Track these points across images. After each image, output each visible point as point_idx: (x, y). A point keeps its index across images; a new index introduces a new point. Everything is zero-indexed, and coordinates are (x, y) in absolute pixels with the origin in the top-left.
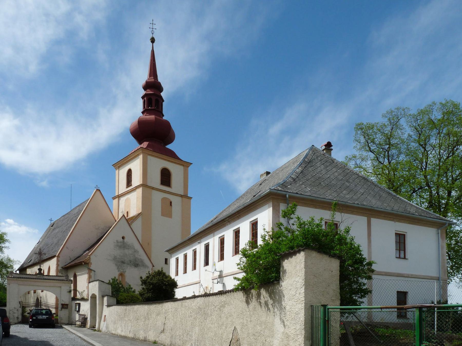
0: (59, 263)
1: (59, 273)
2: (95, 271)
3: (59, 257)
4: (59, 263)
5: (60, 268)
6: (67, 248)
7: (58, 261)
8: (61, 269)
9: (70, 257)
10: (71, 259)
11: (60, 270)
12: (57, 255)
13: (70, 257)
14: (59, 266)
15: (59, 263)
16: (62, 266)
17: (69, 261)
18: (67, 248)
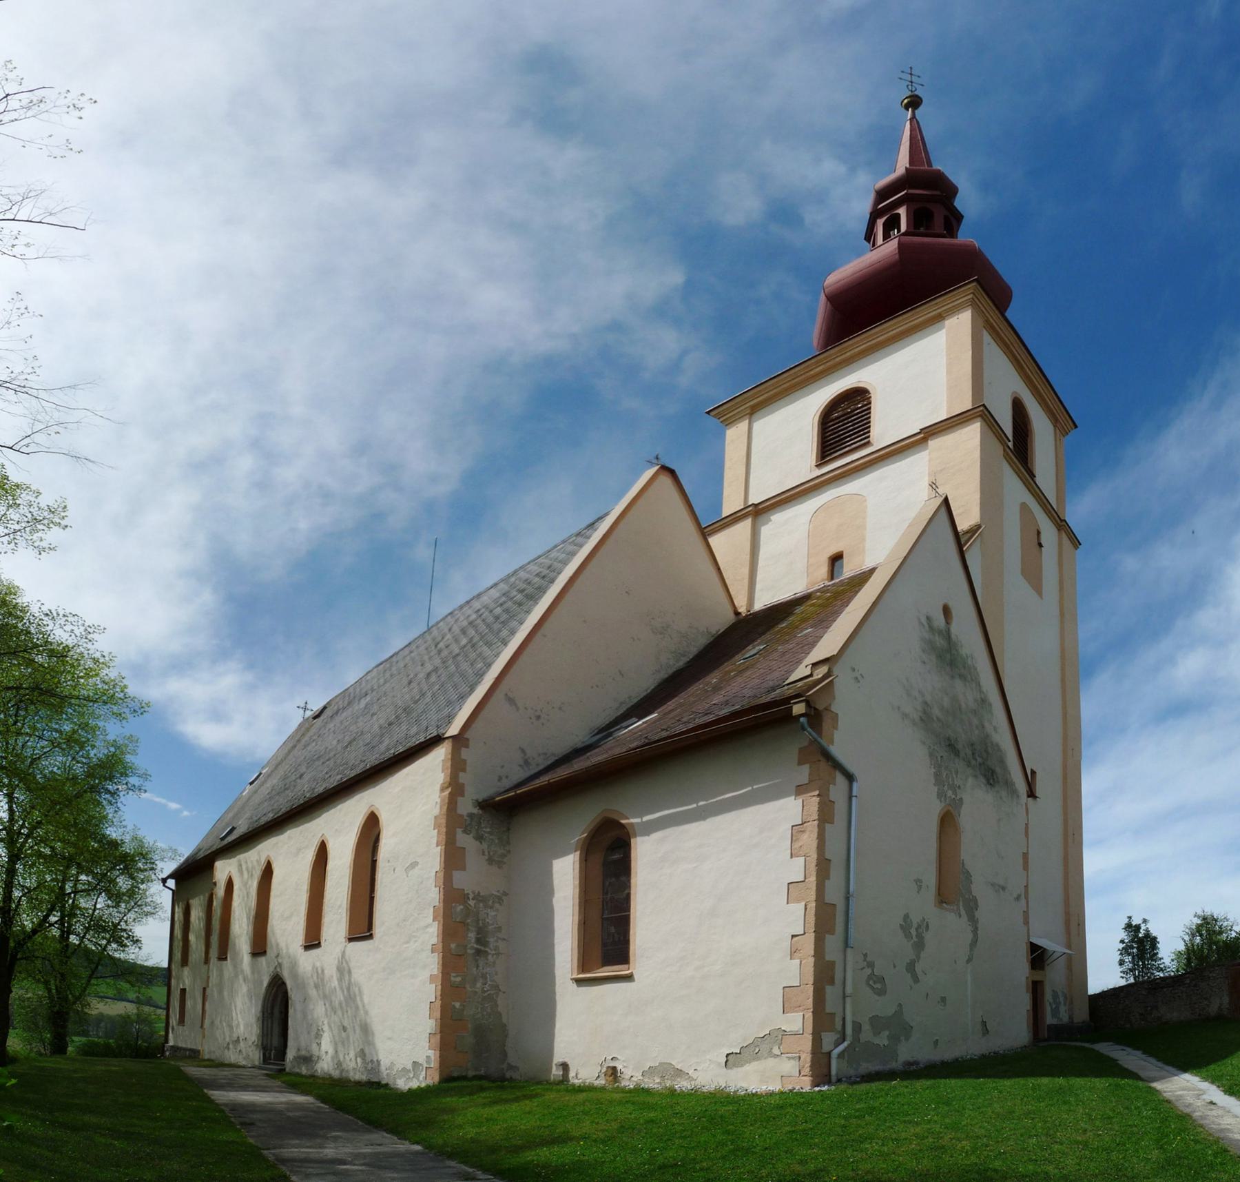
0: (463, 778)
1: (459, 831)
2: (850, 778)
3: (467, 747)
4: (463, 778)
5: (466, 807)
6: (511, 701)
7: (457, 766)
8: (476, 811)
9: (523, 751)
10: (527, 762)
11: (471, 815)
12: (454, 730)
13: (523, 751)
14: (462, 795)
15: (461, 774)
16: (483, 796)
17: (518, 775)
18: (511, 701)
